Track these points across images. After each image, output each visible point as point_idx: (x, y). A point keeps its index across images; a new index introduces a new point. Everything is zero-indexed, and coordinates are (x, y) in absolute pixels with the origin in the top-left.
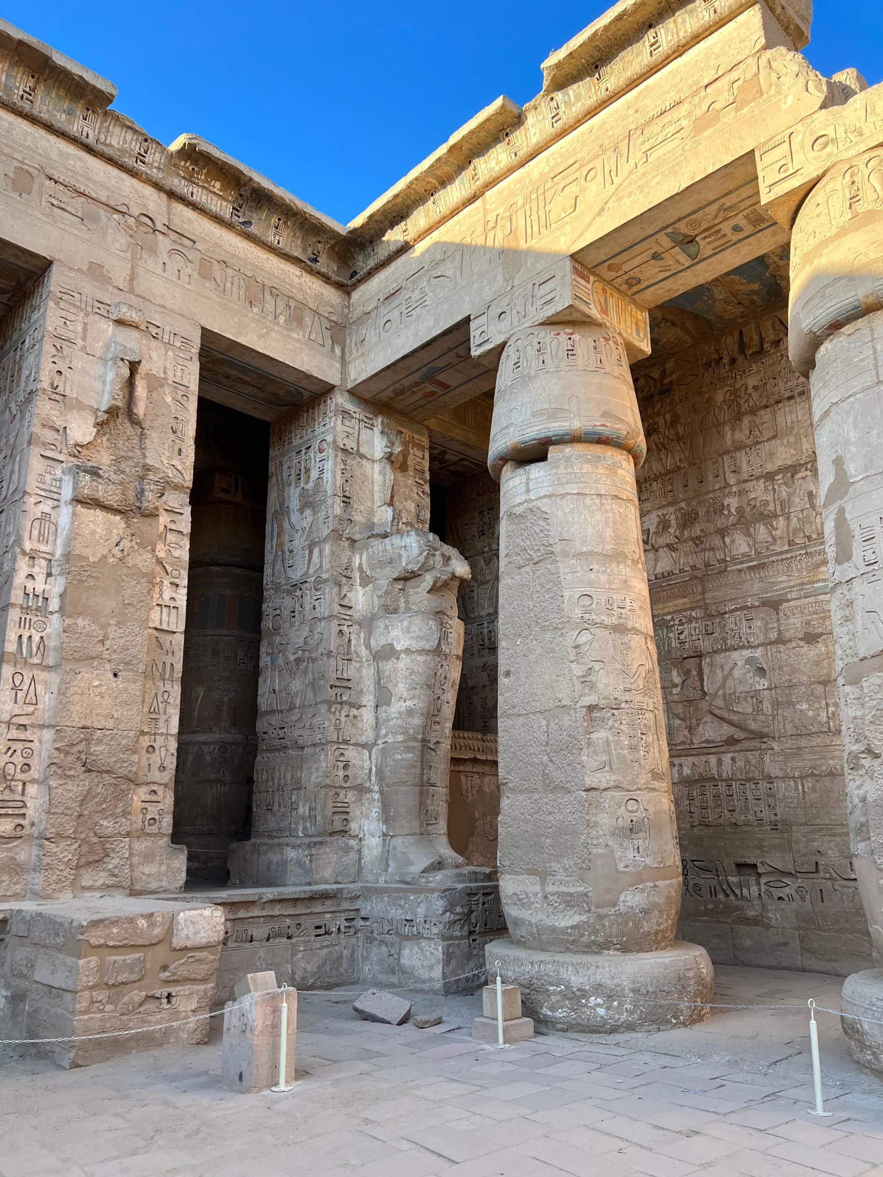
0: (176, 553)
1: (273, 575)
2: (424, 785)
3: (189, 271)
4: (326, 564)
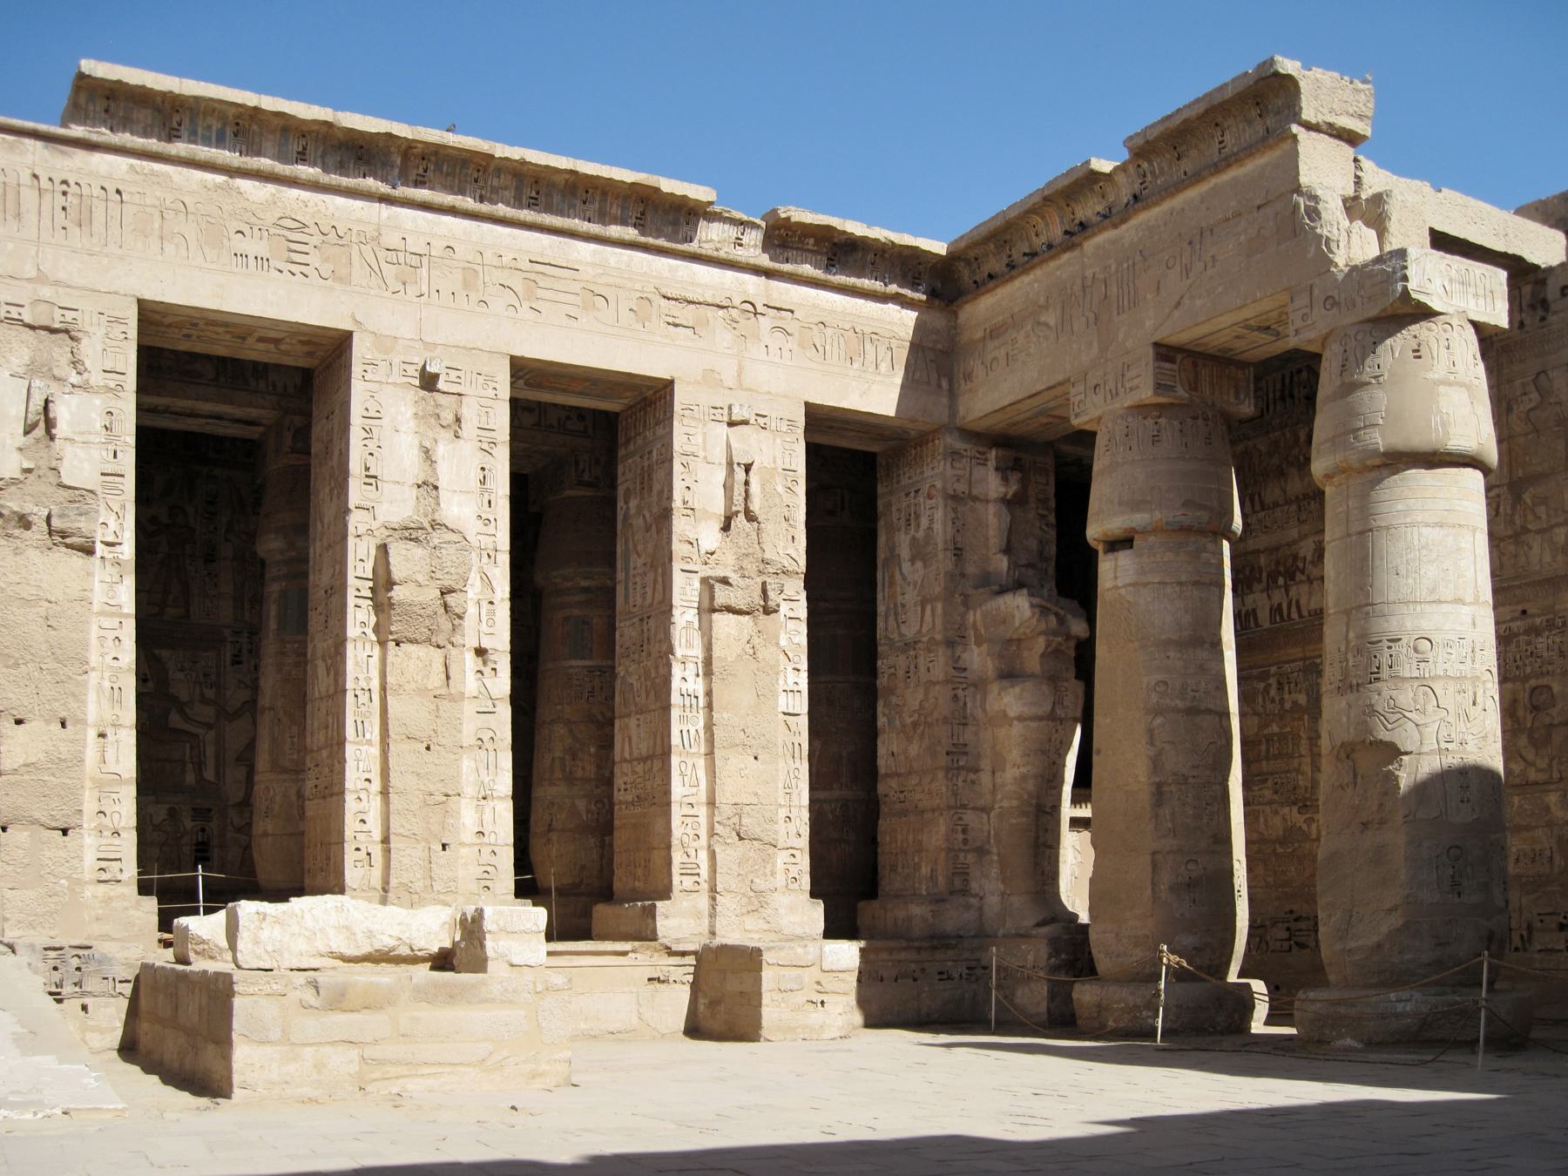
0: (796, 640)
1: (887, 629)
3: (789, 346)
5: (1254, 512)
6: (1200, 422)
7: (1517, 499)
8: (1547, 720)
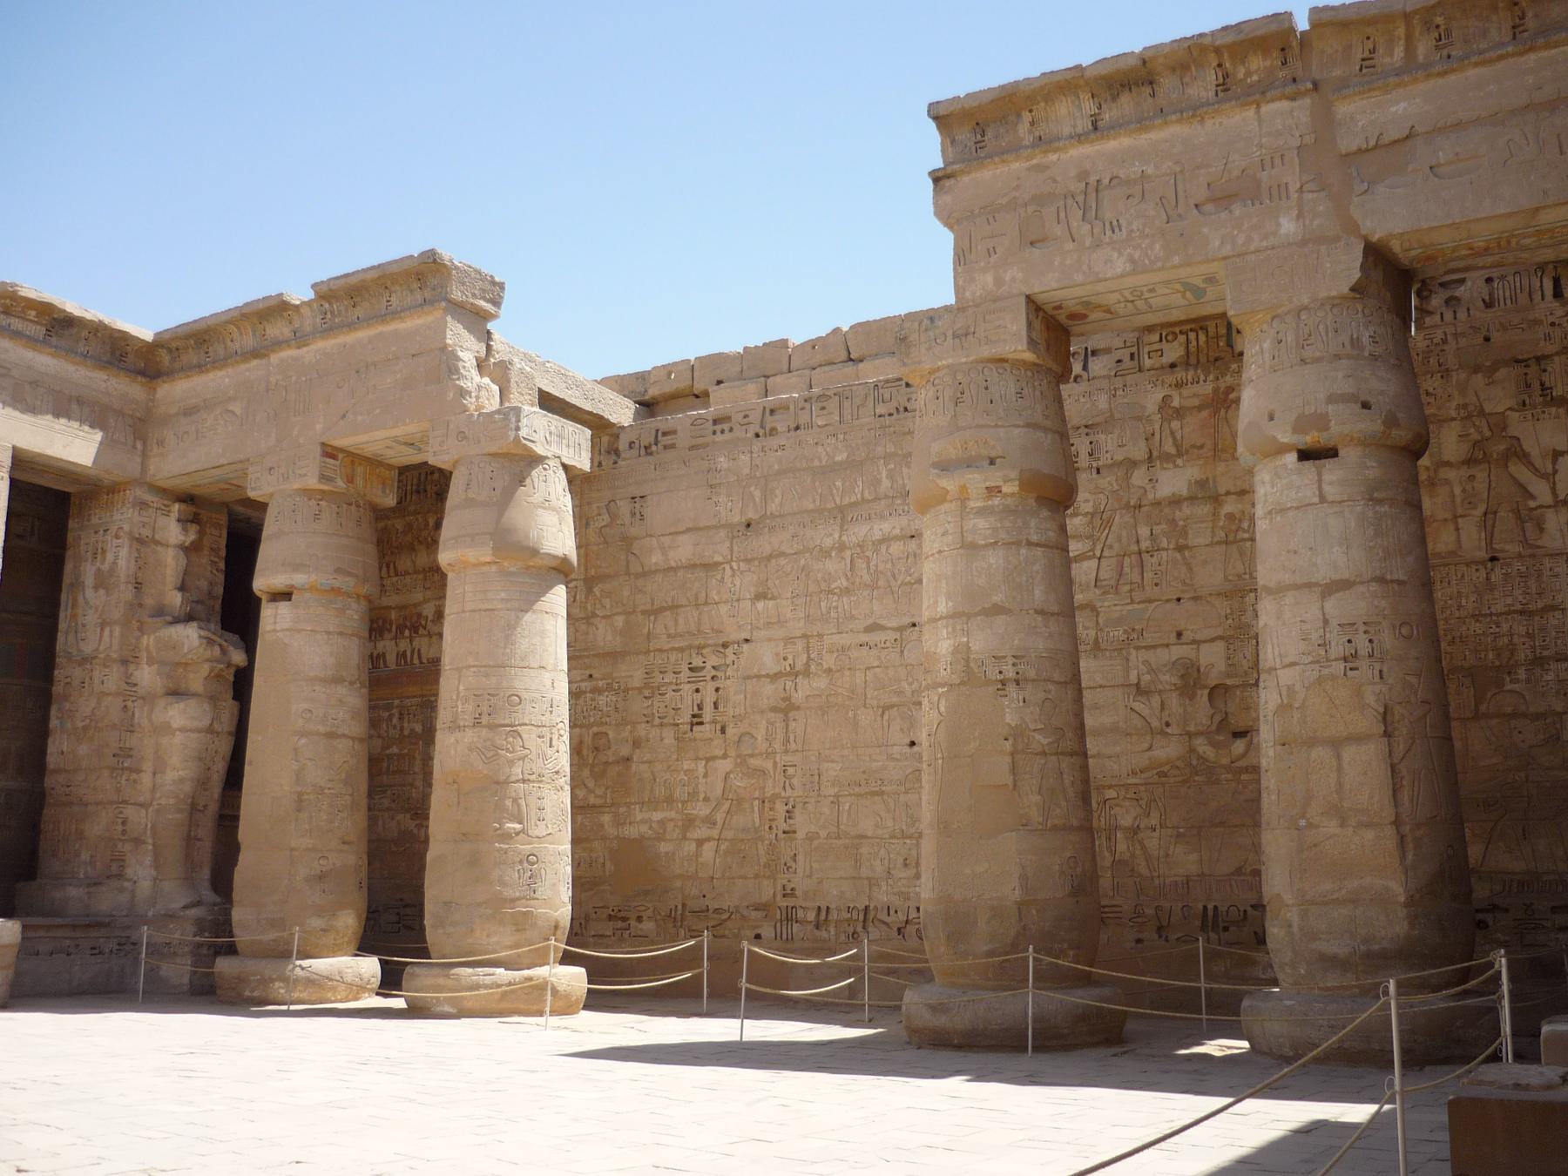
1: (66, 643)
2: (190, 840)
4: (115, 647)
5: (389, 576)
6: (353, 508)
7: (590, 591)
8: (604, 759)
